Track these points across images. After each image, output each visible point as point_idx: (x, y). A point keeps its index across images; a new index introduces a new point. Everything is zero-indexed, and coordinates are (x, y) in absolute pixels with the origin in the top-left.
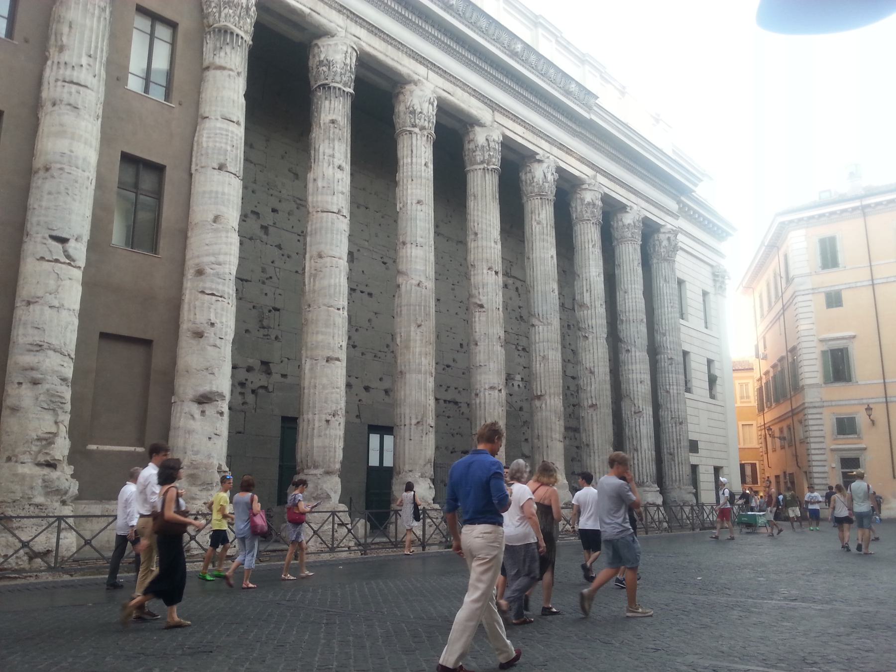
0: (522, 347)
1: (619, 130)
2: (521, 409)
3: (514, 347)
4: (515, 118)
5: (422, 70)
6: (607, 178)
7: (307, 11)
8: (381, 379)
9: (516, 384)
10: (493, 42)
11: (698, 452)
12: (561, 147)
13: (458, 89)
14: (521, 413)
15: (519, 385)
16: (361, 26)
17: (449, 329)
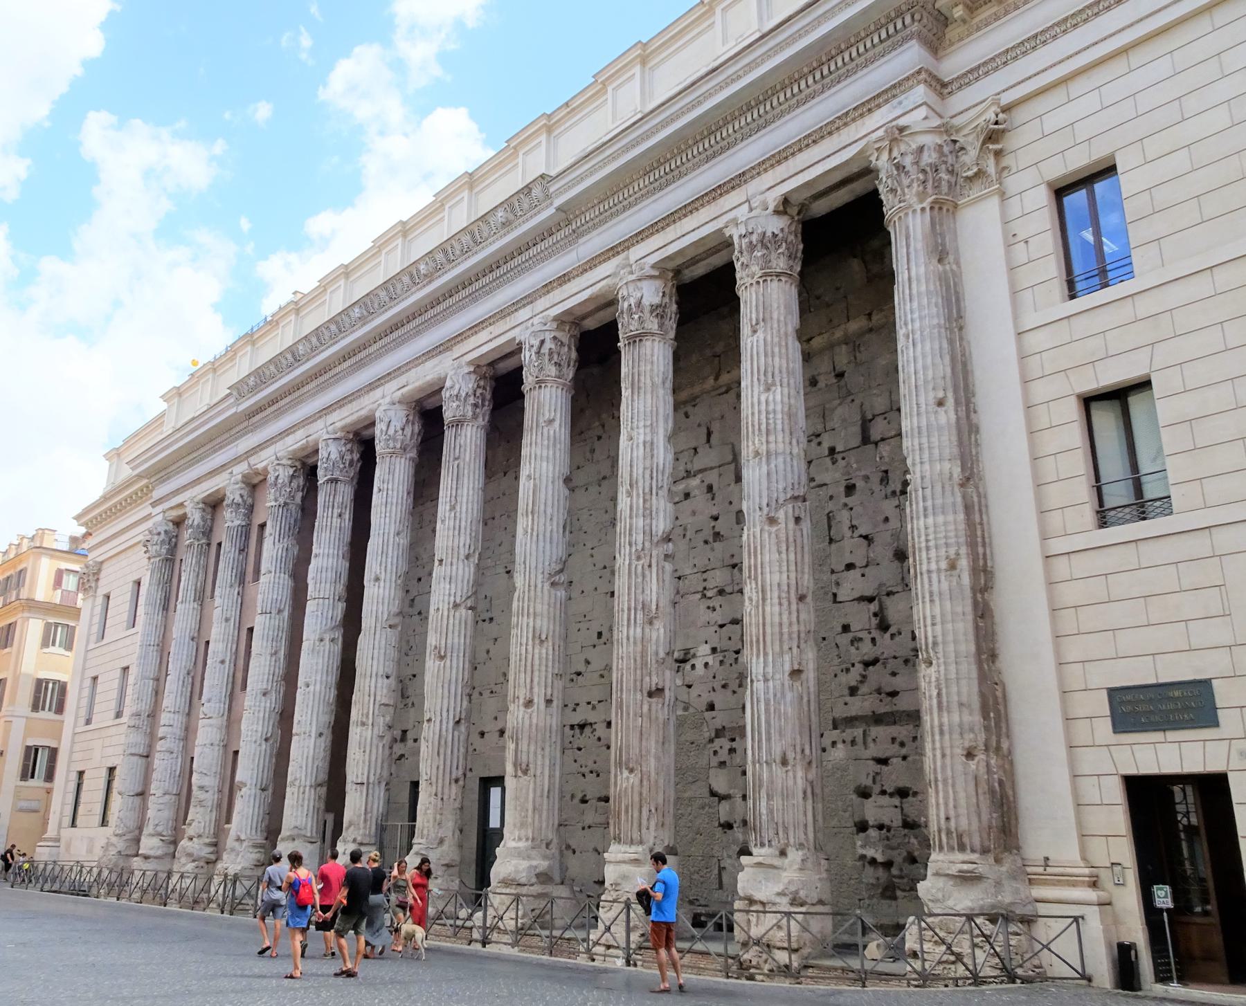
0: (715, 590)
1: (627, 148)
2: (711, 707)
3: (699, 596)
4: (475, 328)
5: (378, 393)
6: (652, 234)
7: (304, 441)
8: (496, 718)
9: (699, 663)
10: (409, 293)
11: (1215, 724)
12: (548, 288)
13: (413, 371)
14: (708, 715)
15: (706, 665)
16: (335, 410)
17: (582, 619)
